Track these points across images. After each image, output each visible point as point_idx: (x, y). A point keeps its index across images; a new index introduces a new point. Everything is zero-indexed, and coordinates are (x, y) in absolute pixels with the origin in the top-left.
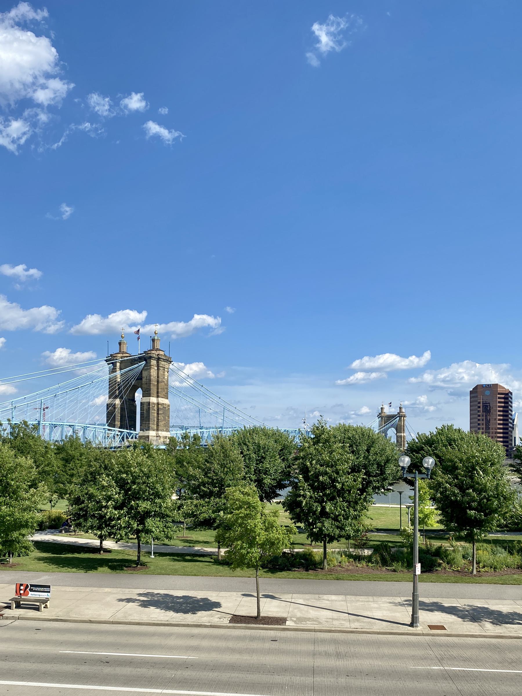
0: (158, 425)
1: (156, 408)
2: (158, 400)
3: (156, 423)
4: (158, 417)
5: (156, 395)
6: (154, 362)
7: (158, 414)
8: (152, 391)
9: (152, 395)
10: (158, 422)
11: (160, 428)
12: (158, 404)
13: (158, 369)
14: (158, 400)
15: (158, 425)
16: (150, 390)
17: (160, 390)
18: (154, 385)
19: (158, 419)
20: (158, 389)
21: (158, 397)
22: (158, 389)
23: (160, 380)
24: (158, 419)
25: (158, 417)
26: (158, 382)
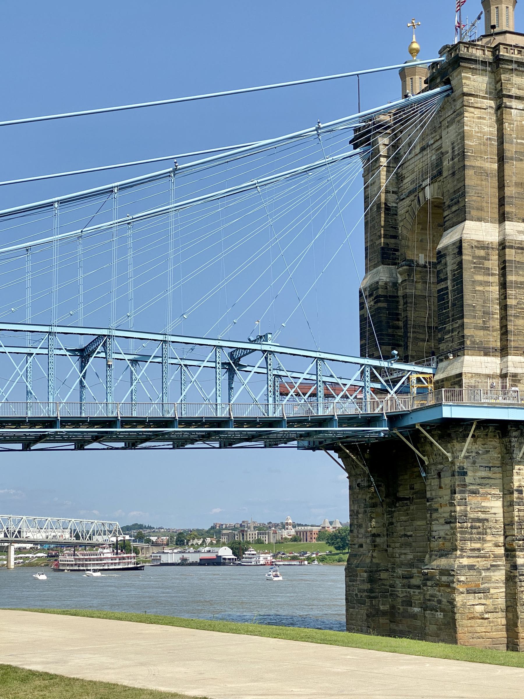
0: (504, 332)
1: (493, 263)
2: (502, 232)
3: (496, 324)
4: (504, 296)
5: (493, 211)
6: (475, 82)
7: (503, 285)
8: (471, 198)
9: (474, 213)
10: (504, 318)
11: (513, 341)
12: (503, 246)
13: (500, 108)
14: (502, 232)
15: (504, 332)
16: (463, 195)
17: (509, 191)
18: (482, 172)
19: (504, 308)
20: (501, 186)
21: (502, 218)
22: (501, 186)
23: (510, 149)
24: (504, 308)
25: (504, 296)
26: (501, 159)
